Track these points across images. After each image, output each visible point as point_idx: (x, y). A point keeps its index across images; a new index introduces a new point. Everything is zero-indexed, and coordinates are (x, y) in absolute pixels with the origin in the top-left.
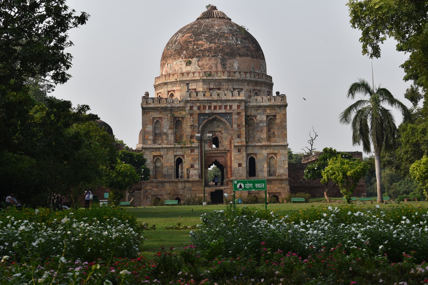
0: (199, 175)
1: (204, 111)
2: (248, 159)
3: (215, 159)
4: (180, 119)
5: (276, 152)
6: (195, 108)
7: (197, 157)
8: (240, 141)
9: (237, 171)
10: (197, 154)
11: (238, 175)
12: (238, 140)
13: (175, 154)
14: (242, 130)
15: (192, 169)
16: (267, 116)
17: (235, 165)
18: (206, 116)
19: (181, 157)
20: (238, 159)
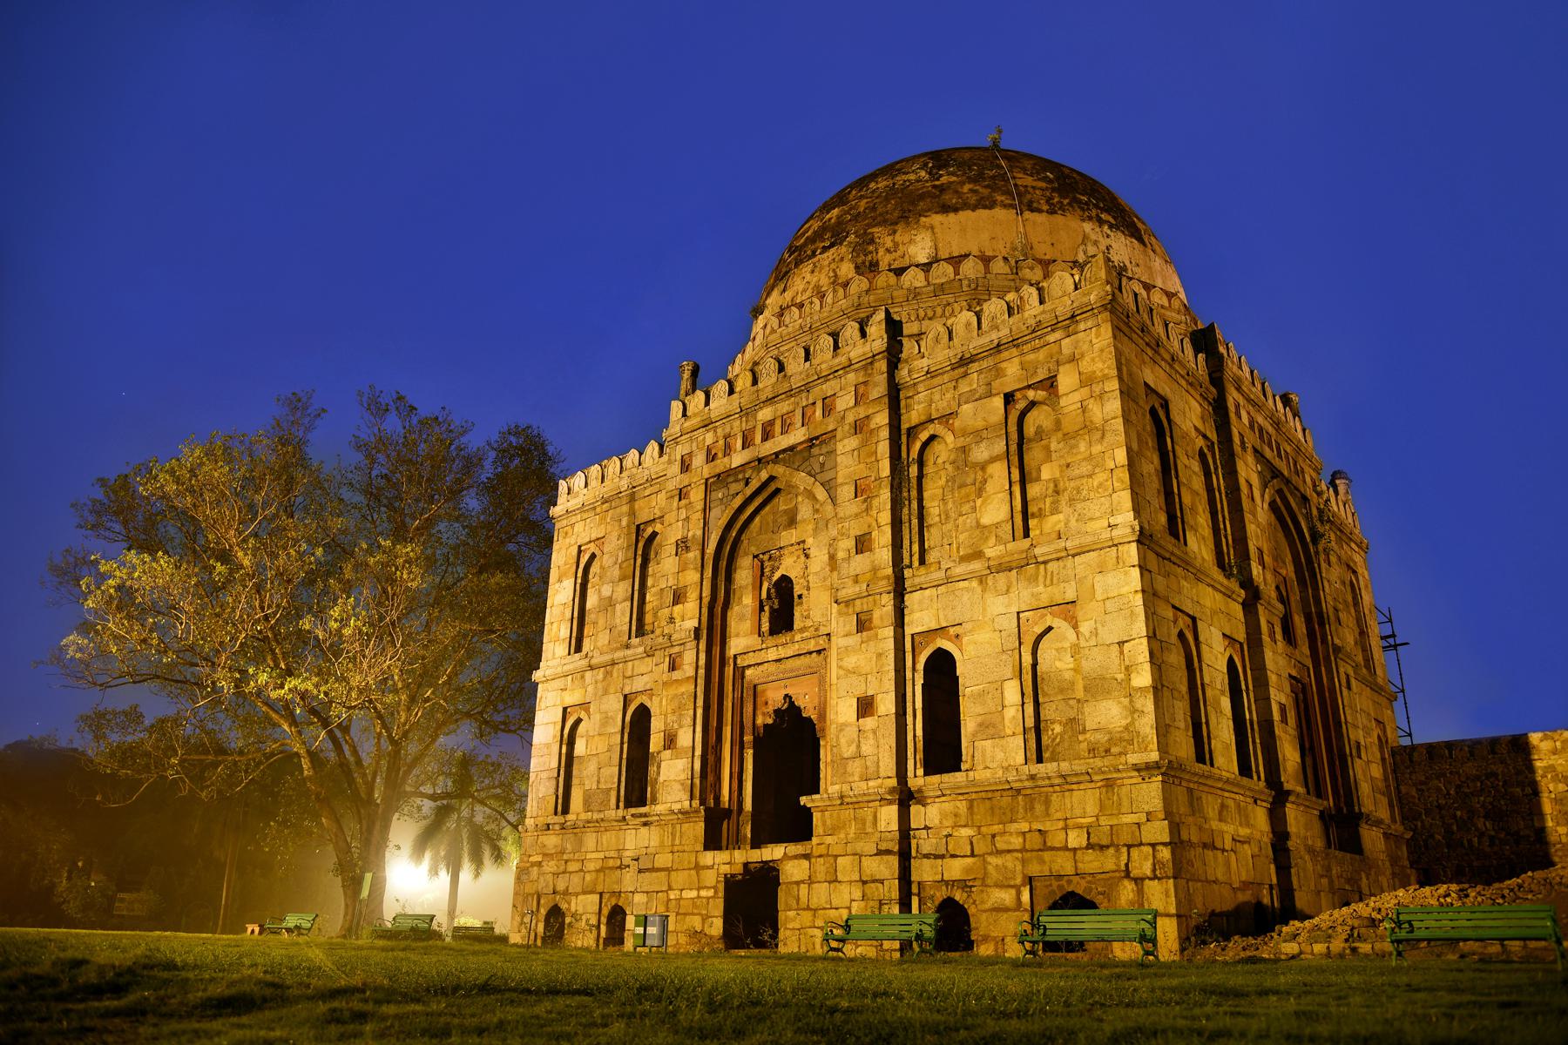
1: (726, 459)
5: (1070, 596)
6: (699, 460)
10: (690, 672)
15: (668, 752)
16: (1009, 398)
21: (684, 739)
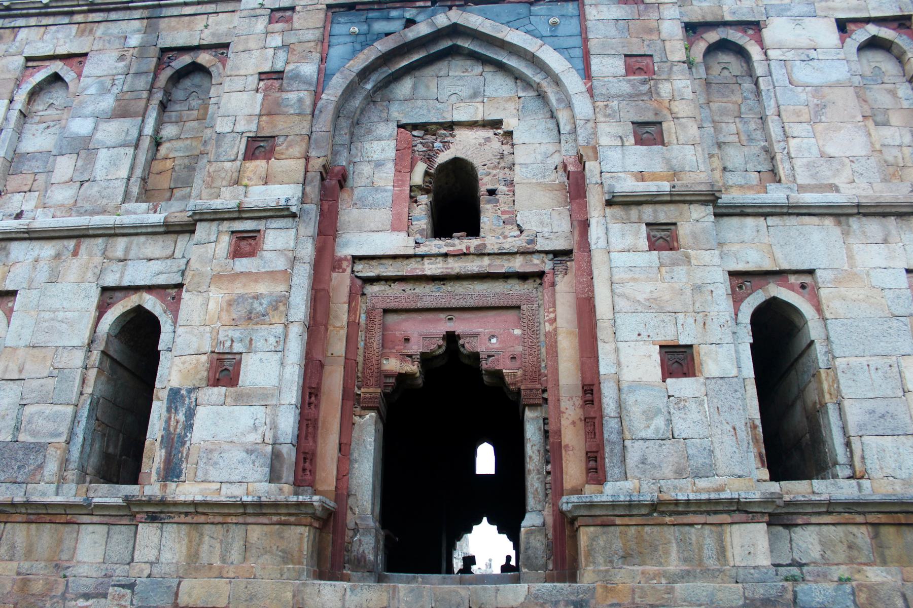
0: (276, 456)
2: (746, 316)
3: (442, 326)
4: (204, 58)
7: (280, 288)
8: (658, 166)
9: (650, 414)
11: (666, 457)
12: (640, 157)
13: (111, 280)
14: (665, 89)
16: (843, 26)
17: (629, 362)
18: (388, 19)
19: (151, 303)
20: (654, 305)
21: (257, 371)
